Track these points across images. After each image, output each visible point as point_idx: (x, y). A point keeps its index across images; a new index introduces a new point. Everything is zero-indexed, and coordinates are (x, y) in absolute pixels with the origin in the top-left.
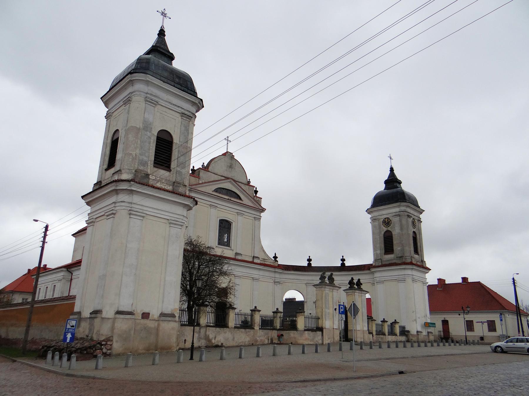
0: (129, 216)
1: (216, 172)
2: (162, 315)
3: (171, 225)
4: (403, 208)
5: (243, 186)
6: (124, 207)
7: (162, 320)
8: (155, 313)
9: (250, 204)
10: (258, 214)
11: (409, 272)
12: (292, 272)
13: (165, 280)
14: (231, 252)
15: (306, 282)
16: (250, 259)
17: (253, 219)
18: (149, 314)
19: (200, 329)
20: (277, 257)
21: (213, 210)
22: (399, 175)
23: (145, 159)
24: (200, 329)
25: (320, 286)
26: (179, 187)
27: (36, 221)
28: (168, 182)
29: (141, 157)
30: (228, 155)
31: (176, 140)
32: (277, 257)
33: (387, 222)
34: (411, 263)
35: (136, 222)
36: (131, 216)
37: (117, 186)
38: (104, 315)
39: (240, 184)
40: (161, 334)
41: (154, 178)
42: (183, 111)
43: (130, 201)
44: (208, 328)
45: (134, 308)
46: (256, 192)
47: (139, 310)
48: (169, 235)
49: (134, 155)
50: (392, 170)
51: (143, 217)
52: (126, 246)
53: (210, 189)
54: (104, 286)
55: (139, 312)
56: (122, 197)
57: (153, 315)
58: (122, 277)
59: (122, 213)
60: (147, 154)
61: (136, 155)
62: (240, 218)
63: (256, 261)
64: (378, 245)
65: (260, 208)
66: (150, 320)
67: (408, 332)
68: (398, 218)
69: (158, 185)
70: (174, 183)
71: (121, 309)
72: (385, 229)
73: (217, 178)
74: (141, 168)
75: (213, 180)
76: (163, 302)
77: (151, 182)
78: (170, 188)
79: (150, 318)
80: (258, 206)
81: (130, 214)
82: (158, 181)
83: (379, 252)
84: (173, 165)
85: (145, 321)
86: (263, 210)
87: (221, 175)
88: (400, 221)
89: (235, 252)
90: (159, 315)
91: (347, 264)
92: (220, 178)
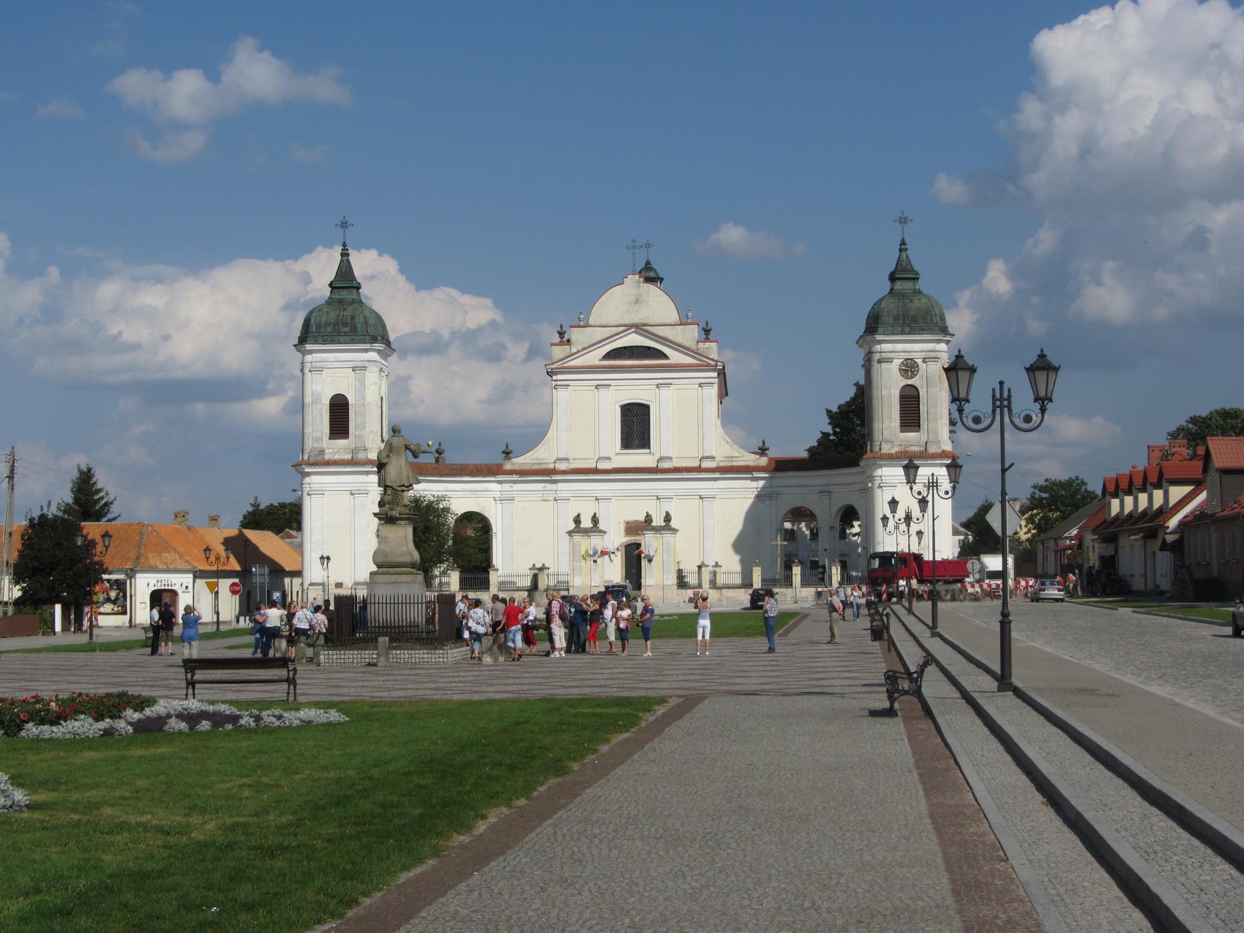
1: (604, 323)
14: (649, 457)
16: (696, 464)
23: (319, 434)
28: (346, 450)
42: (355, 364)
53: (594, 358)
62: (664, 391)
63: (705, 464)
69: (337, 457)
73: (607, 332)
74: (316, 445)
75: (599, 338)
77: (327, 457)
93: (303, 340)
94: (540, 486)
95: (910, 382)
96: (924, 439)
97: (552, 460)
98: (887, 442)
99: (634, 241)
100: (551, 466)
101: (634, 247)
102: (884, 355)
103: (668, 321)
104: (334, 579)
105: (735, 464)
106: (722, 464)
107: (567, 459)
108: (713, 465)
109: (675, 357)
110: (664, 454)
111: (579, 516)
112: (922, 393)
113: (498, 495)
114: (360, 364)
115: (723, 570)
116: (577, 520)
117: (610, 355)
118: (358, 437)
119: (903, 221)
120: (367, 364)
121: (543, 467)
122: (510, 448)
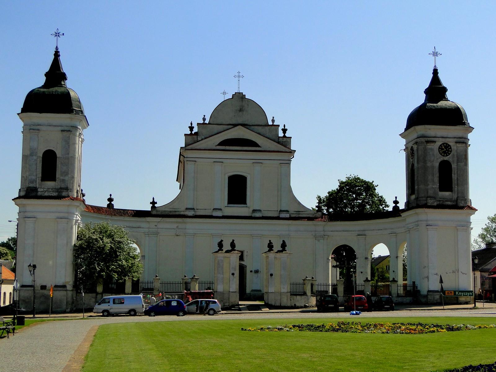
1: (219, 122)
15: (357, 233)
16: (276, 215)
19: (97, 295)
21: (218, 167)
23: (34, 177)
26: (62, 192)
27: (10, 221)
29: (30, 177)
30: (240, 97)
31: (59, 154)
34: (426, 206)
41: (42, 190)
42: (62, 128)
46: (284, 131)
49: (25, 177)
50: (435, 72)
60: (35, 174)
61: (26, 176)
63: (283, 215)
65: (287, 150)
66: (48, 290)
69: (46, 194)
71: (25, 284)
73: (221, 128)
74: (31, 185)
75: (216, 132)
77: (39, 194)
78: (55, 194)
79: (47, 289)
82: (46, 191)
84: (58, 175)
85: (43, 291)
86: (292, 152)
87: (228, 123)
89: (251, 210)
93: (24, 110)
94: (175, 226)
95: (446, 158)
96: (455, 197)
97: (183, 209)
98: (431, 197)
99: (239, 72)
100: (182, 213)
101: (239, 76)
102: (429, 139)
103: (260, 124)
104: (38, 284)
105: (301, 216)
106: (293, 216)
107: (193, 209)
108: (287, 216)
110: (257, 208)
111: (222, 241)
112: (454, 166)
113: (147, 230)
114: (66, 128)
115: (317, 283)
116: (220, 245)
117: (223, 143)
118: (63, 181)
119: (435, 54)
120: (71, 129)
121: (177, 213)
122: (155, 201)
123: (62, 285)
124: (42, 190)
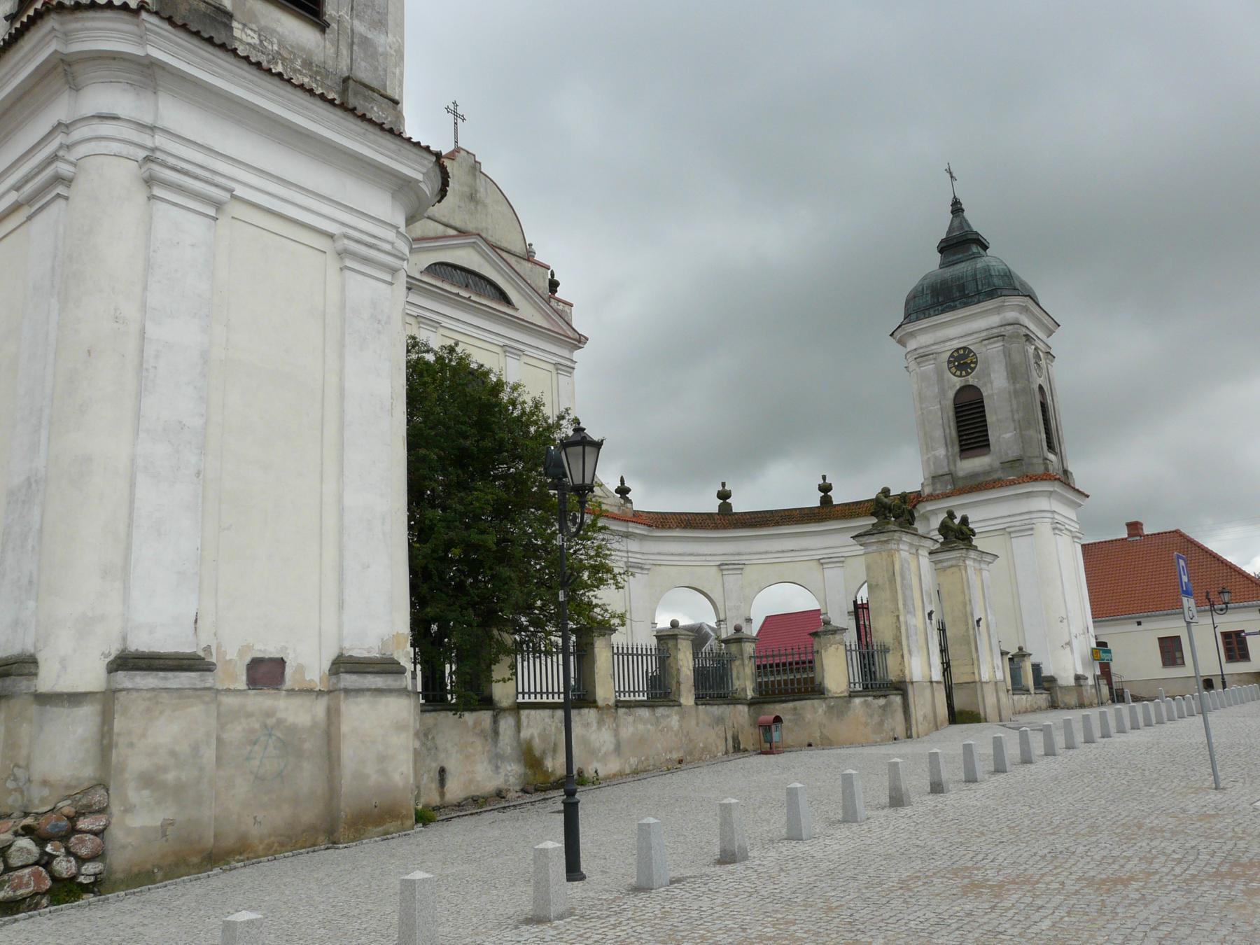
0: (140, 195)
2: (344, 665)
3: (349, 263)
4: (1011, 315)
5: (512, 260)
6: (115, 147)
7: (347, 691)
8: (309, 661)
9: (539, 320)
10: (566, 353)
11: (1043, 504)
12: (677, 533)
13: (341, 511)
17: (551, 367)
18: (281, 662)
19: (495, 721)
20: (628, 490)
22: (977, 221)
24: (495, 721)
25: (883, 537)
32: (628, 490)
33: (962, 361)
35: (180, 226)
36: (157, 191)
37: (67, 37)
38: (49, 679)
39: (505, 255)
40: (348, 753)
43: (148, 119)
44: (524, 713)
45: (205, 639)
46: (554, 285)
47: (234, 646)
48: (343, 306)
50: (957, 208)
51: (219, 205)
52: (143, 332)
54: (41, 531)
55: (232, 654)
56: (103, 97)
57: (301, 669)
58: (132, 485)
59: (108, 174)
64: (938, 433)
65: (570, 333)
66: (291, 692)
67: (1052, 680)
68: (997, 347)
70: (346, 80)
71: (142, 643)
72: (957, 382)
76: (341, 606)
79: (289, 681)
80: (565, 327)
81: (149, 181)
83: (941, 452)
85: (261, 701)
86: (579, 341)
87: (445, 220)
88: (1007, 354)
90: (326, 665)
91: (838, 497)
92: (440, 229)
109: (526, 310)
123: (375, 654)
124: (249, 40)
